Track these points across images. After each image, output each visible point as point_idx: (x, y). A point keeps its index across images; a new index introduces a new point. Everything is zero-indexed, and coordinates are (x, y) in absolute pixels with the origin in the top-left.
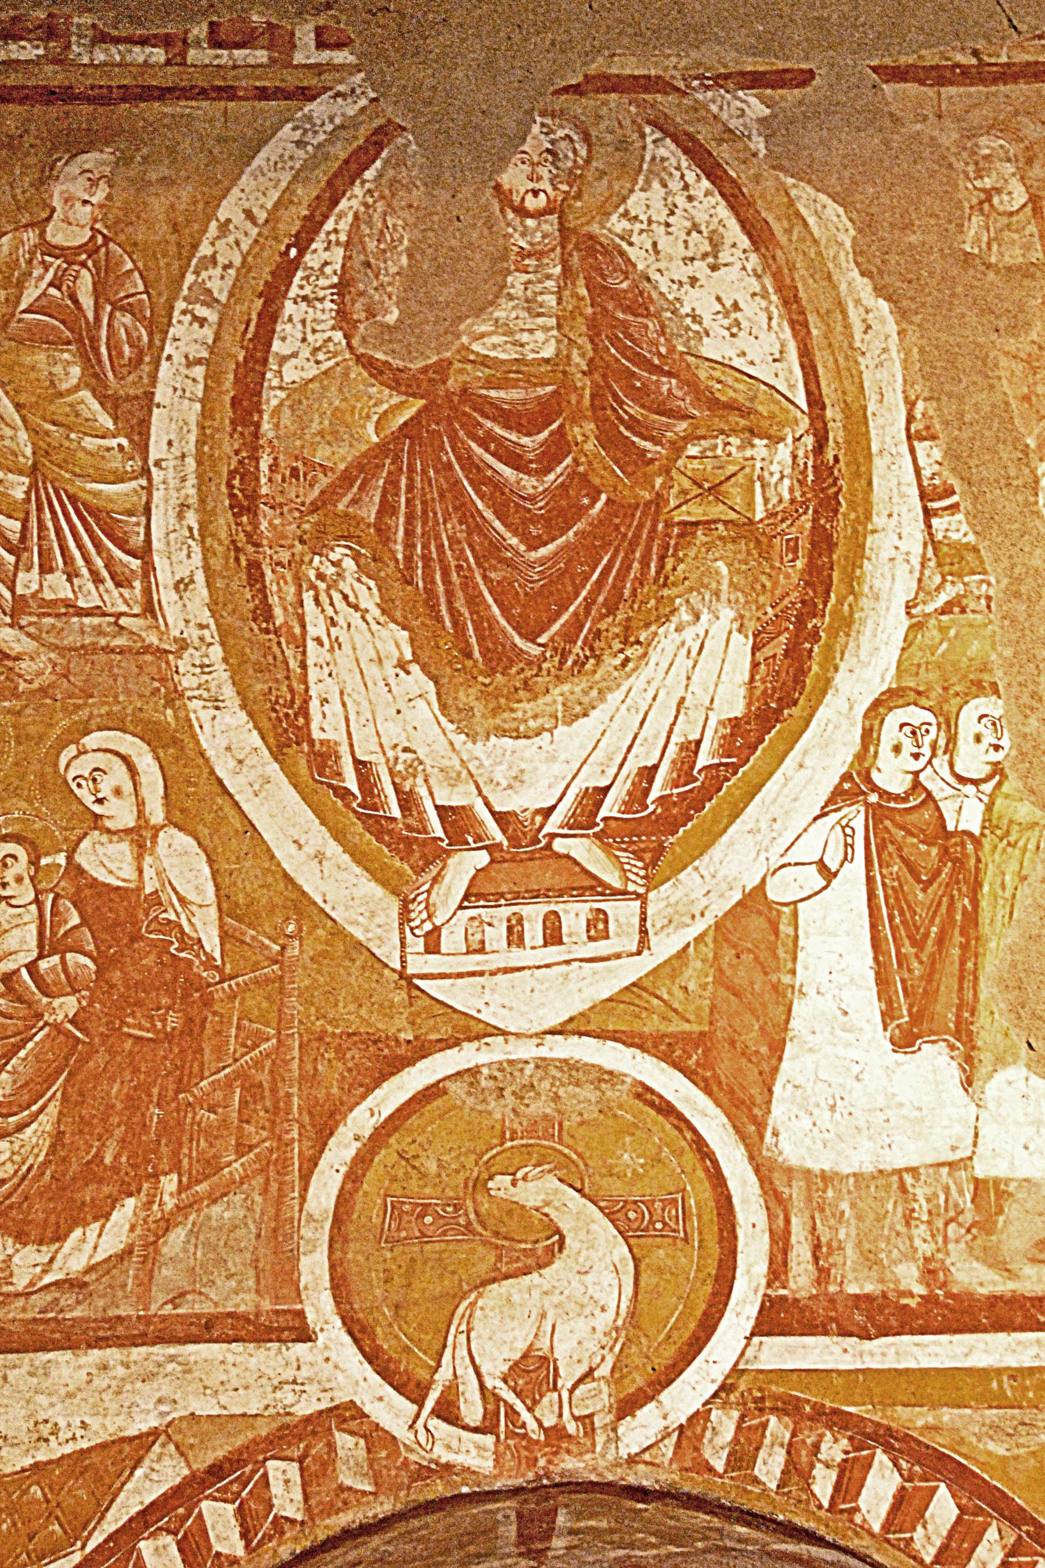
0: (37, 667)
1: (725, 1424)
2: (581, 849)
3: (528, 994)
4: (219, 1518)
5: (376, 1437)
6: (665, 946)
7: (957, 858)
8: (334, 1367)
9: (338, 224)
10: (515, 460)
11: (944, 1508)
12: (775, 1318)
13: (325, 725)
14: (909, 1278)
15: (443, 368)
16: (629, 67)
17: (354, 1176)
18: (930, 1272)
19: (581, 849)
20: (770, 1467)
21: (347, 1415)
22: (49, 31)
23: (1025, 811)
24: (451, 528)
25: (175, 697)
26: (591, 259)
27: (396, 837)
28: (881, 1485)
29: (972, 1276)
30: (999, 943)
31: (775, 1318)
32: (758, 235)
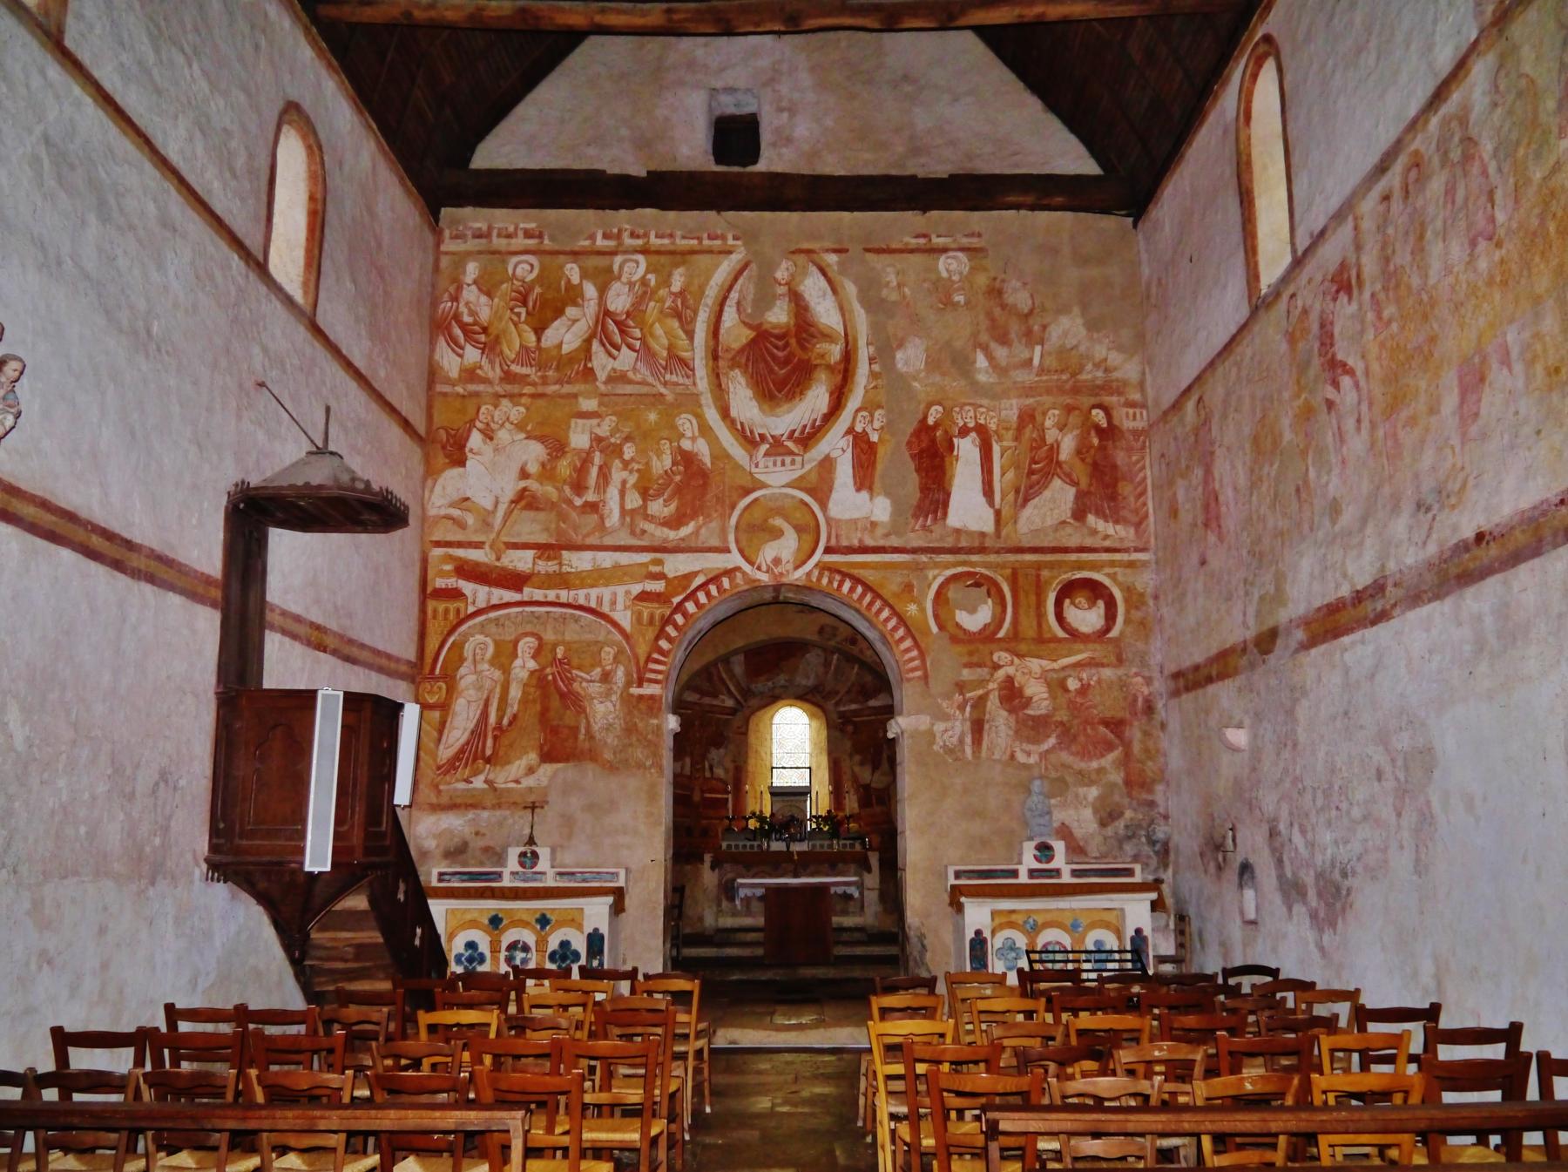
0: (670, 397)
1: (816, 573)
2: (790, 444)
3: (777, 478)
4: (713, 589)
5: (744, 573)
6: (808, 467)
7: (872, 447)
8: (735, 559)
9: (737, 287)
10: (777, 347)
11: (860, 589)
12: (828, 550)
13: (734, 413)
14: (856, 543)
15: (761, 324)
16: (805, 246)
17: (741, 516)
18: (860, 541)
19: (790, 444)
20: (825, 581)
21: (738, 569)
22: (671, 236)
23: (887, 437)
24: (762, 365)
25: (700, 406)
26: (797, 299)
27: (750, 440)
28: (847, 585)
29: (869, 542)
30: (880, 467)
31: (828, 550)
32: (834, 291)
